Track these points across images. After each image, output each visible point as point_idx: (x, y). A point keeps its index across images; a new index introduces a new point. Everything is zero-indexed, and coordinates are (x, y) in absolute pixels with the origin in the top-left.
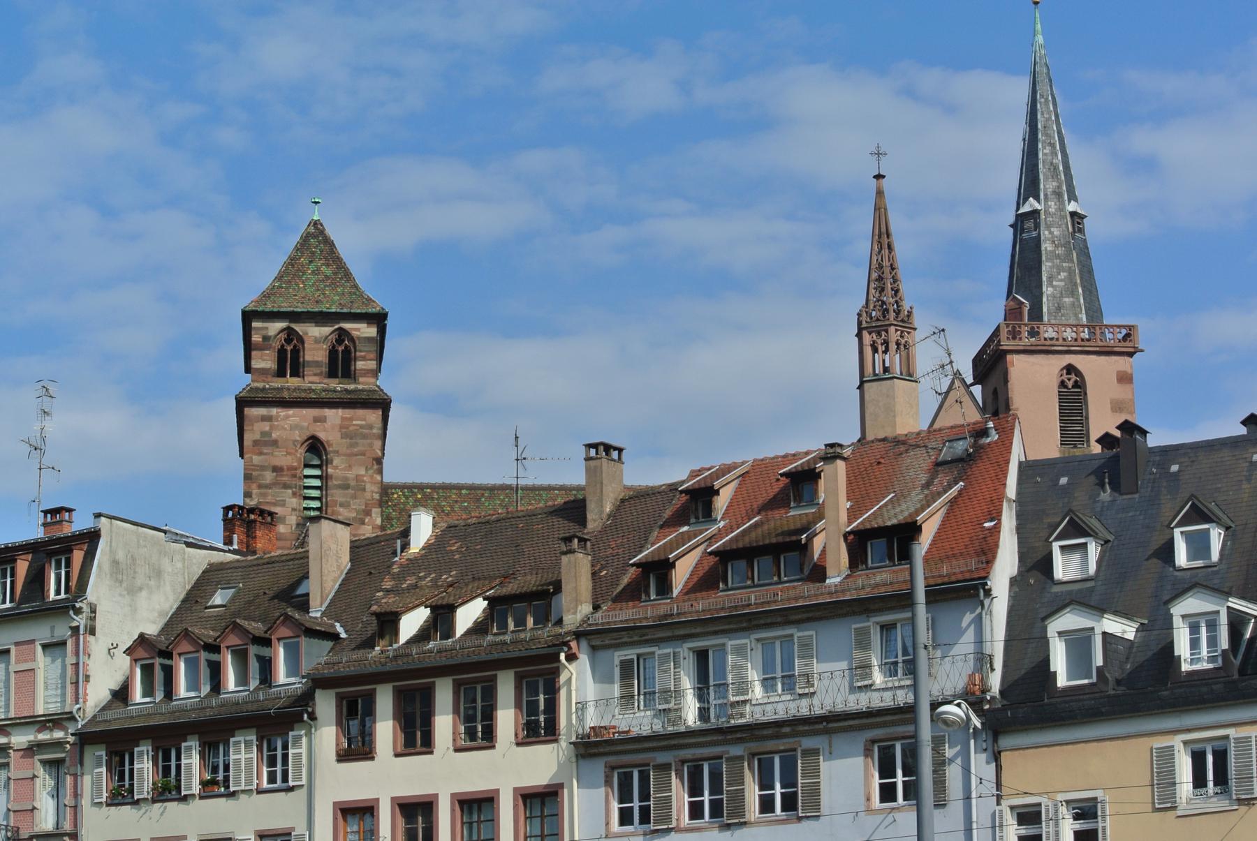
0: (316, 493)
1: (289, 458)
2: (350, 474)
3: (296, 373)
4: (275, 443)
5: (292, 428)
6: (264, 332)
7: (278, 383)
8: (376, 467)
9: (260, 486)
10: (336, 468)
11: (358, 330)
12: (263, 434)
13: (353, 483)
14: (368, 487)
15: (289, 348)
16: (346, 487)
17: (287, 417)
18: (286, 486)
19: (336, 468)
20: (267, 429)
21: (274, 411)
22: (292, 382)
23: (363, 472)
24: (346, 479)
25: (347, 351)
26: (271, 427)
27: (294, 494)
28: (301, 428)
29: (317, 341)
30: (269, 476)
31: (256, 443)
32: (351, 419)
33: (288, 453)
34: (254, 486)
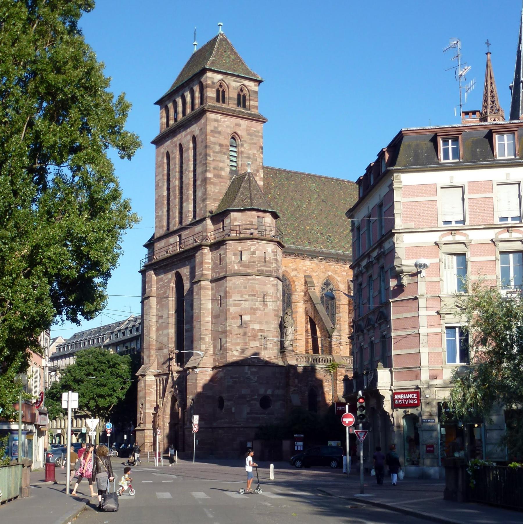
0: (234, 159)
1: (226, 140)
2: (251, 152)
3: (224, 102)
4: (220, 133)
5: (228, 127)
6: (212, 80)
7: (217, 105)
8: (261, 151)
9: (214, 152)
10: (245, 148)
11: (251, 86)
12: (215, 127)
13: (252, 157)
14: (258, 159)
15: (221, 90)
16: (249, 158)
17: (225, 121)
18: (225, 154)
19: (245, 148)
20: (216, 125)
21: (219, 117)
22: (224, 106)
23: (255, 152)
24: (249, 154)
25: (244, 96)
26: (218, 125)
27: (228, 158)
28: (231, 128)
29: (234, 88)
30: (217, 148)
31: (212, 131)
32: (251, 127)
33: (225, 138)
34: (211, 151)
